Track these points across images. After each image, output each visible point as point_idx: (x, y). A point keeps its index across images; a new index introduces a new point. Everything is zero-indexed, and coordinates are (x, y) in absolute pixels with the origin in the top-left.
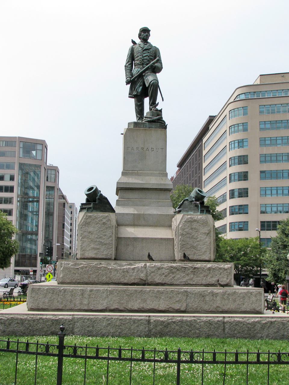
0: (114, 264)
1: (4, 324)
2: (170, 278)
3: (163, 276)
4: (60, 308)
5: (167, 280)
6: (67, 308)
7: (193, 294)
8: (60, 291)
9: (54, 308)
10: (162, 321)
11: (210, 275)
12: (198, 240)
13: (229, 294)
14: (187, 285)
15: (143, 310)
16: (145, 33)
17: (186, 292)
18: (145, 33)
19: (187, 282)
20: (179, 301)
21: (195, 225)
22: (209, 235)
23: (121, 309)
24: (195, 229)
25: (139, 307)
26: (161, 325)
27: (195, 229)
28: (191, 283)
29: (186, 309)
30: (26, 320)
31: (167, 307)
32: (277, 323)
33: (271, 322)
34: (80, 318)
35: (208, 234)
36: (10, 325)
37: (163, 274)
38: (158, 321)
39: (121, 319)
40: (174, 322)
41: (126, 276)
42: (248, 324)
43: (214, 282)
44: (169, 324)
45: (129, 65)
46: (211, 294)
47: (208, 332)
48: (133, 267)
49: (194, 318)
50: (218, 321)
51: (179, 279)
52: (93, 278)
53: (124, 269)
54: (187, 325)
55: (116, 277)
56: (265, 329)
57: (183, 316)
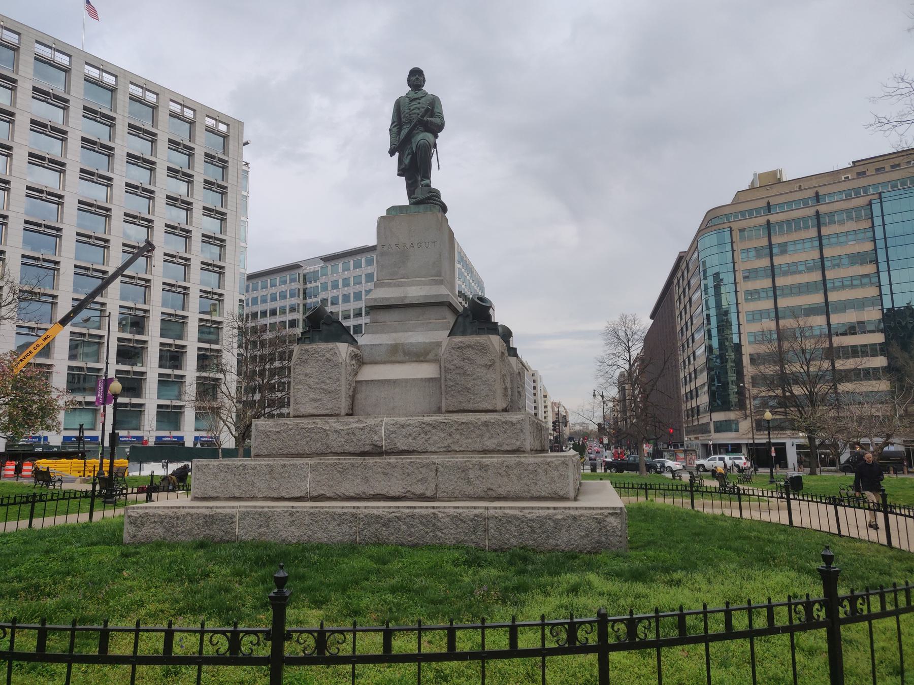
0: (335, 423)
1: (135, 524)
2: (421, 442)
3: (410, 438)
4: (237, 495)
5: (418, 444)
6: (248, 496)
7: (446, 467)
8: (238, 468)
9: (227, 496)
10: (378, 517)
11: (488, 435)
12: (474, 376)
13: (507, 466)
14: (449, 452)
15: (364, 496)
16: (416, 78)
17: (434, 463)
18: (416, 78)
19: (449, 446)
20: (423, 480)
21: (469, 353)
22: (491, 368)
23: (328, 495)
24: (468, 359)
25: (357, 492)
26: (378, 522)
27: (468, 359)
28: (457, 449)
29: (435, 494)
30: (166, 516)
31: (403, 491)
32: (586, 518)
33: (575, 518)
34: (247, 512)
35: (490, 366)
36: (143, 525)
37: (410, 435)
38: (372, 516)
39: (311, 513)
40: (399, 518)
41: (352, 442)
42: (531, 520)
43: (494, 446)
44: (389, 520)
45: (394, 127)
46: (476, 467)
47: (458, 536)
48: (361, 426)
49: (433, 511)
50: (476, 515)
51: (435, 442)
52: (303, 446)
53: (349, 429)
54: (421, 523)
55: (336, 443)
56: (563, 531)
57: (415, 508)
